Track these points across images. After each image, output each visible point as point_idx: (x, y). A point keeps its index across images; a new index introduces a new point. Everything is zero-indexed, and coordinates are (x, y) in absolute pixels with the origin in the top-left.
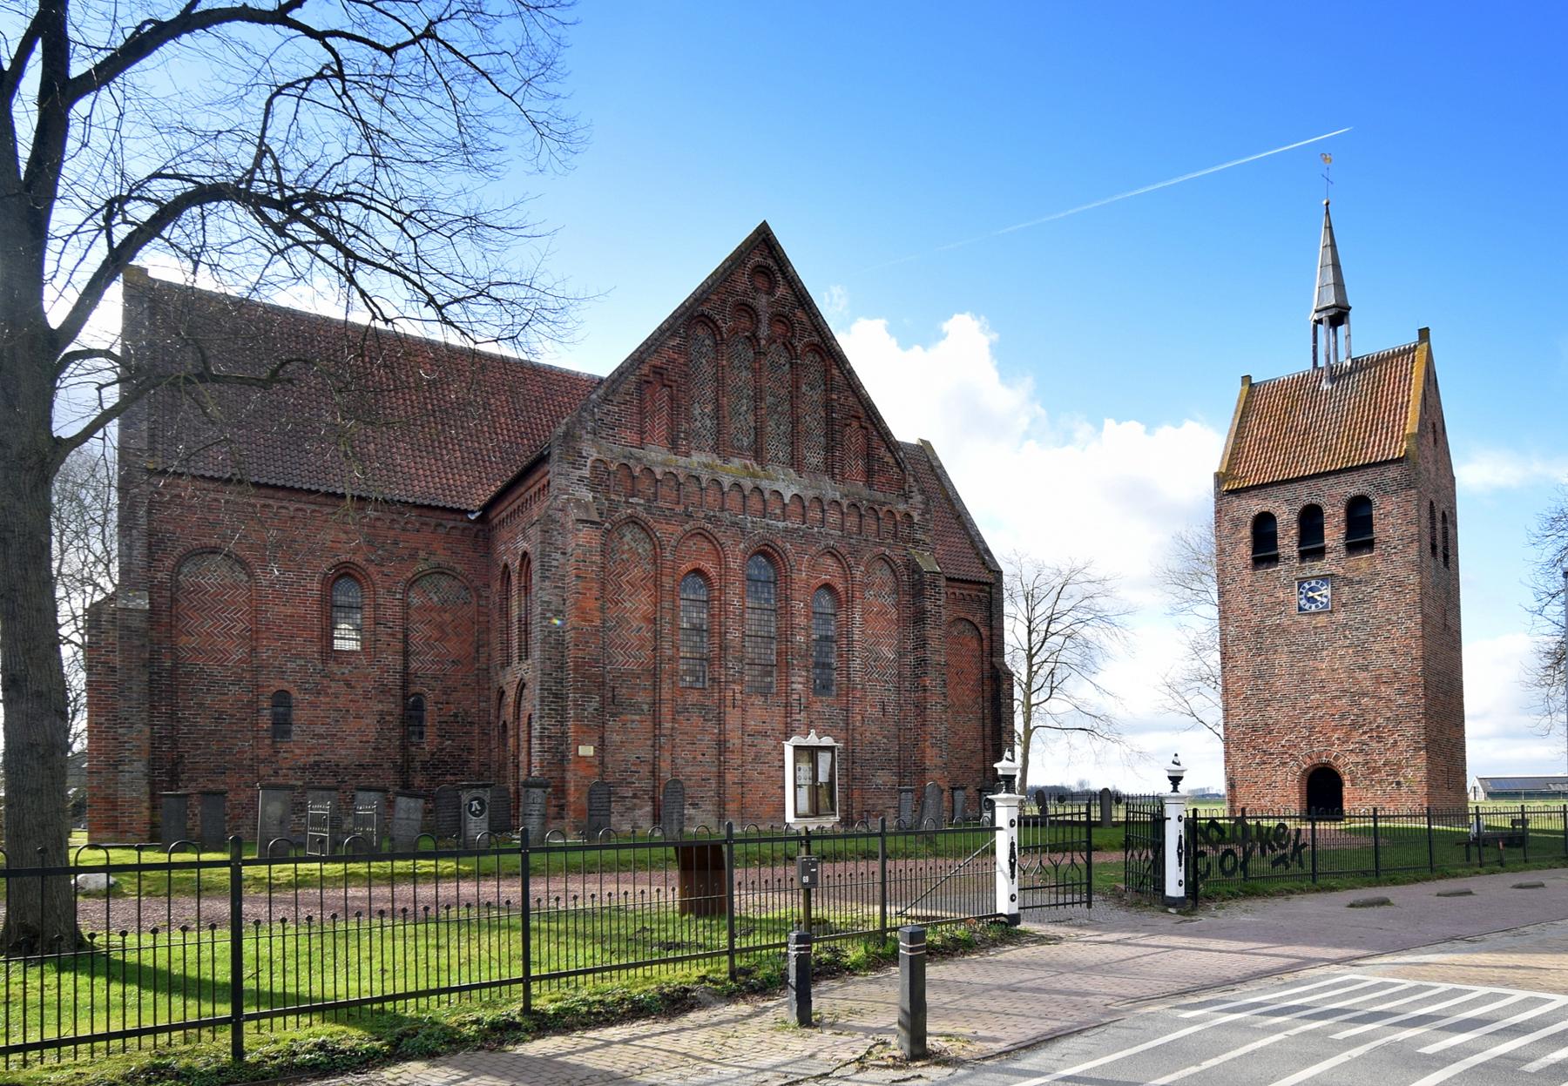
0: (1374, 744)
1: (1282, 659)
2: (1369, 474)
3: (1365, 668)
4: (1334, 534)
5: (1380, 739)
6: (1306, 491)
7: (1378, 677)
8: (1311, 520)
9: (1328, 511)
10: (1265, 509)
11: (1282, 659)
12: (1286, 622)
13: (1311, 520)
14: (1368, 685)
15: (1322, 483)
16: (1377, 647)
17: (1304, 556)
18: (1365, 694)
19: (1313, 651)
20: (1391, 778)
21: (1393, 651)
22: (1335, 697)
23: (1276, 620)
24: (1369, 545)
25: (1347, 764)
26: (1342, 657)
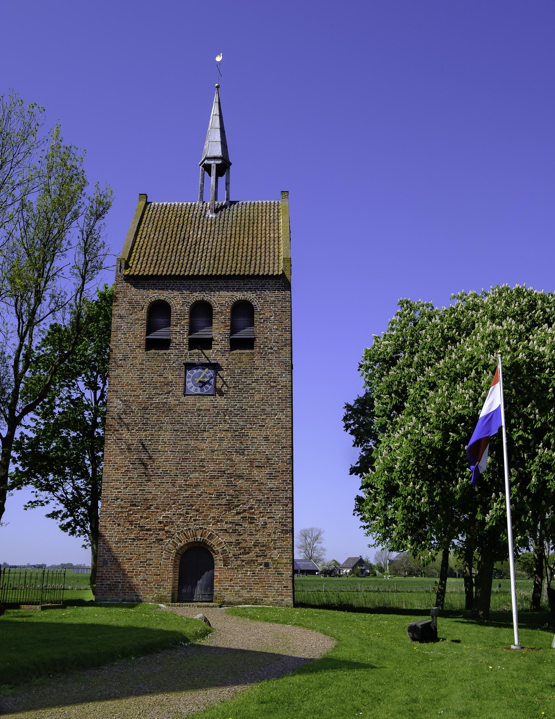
0: (246, 525)
1: (166, 436)
5: (252, 521)
7: (251, 462)
8: (202, 312)
9: (217, 309)
10: (162, 298)
11: (166, 436)
12: (172, 400)
13: (202, 312)
16: (251, 434)
18: (240, 477)
19: (196, 432)
20: (260, 560)
21: (266, 438)
22: (213, 477)
26: (221, 439)
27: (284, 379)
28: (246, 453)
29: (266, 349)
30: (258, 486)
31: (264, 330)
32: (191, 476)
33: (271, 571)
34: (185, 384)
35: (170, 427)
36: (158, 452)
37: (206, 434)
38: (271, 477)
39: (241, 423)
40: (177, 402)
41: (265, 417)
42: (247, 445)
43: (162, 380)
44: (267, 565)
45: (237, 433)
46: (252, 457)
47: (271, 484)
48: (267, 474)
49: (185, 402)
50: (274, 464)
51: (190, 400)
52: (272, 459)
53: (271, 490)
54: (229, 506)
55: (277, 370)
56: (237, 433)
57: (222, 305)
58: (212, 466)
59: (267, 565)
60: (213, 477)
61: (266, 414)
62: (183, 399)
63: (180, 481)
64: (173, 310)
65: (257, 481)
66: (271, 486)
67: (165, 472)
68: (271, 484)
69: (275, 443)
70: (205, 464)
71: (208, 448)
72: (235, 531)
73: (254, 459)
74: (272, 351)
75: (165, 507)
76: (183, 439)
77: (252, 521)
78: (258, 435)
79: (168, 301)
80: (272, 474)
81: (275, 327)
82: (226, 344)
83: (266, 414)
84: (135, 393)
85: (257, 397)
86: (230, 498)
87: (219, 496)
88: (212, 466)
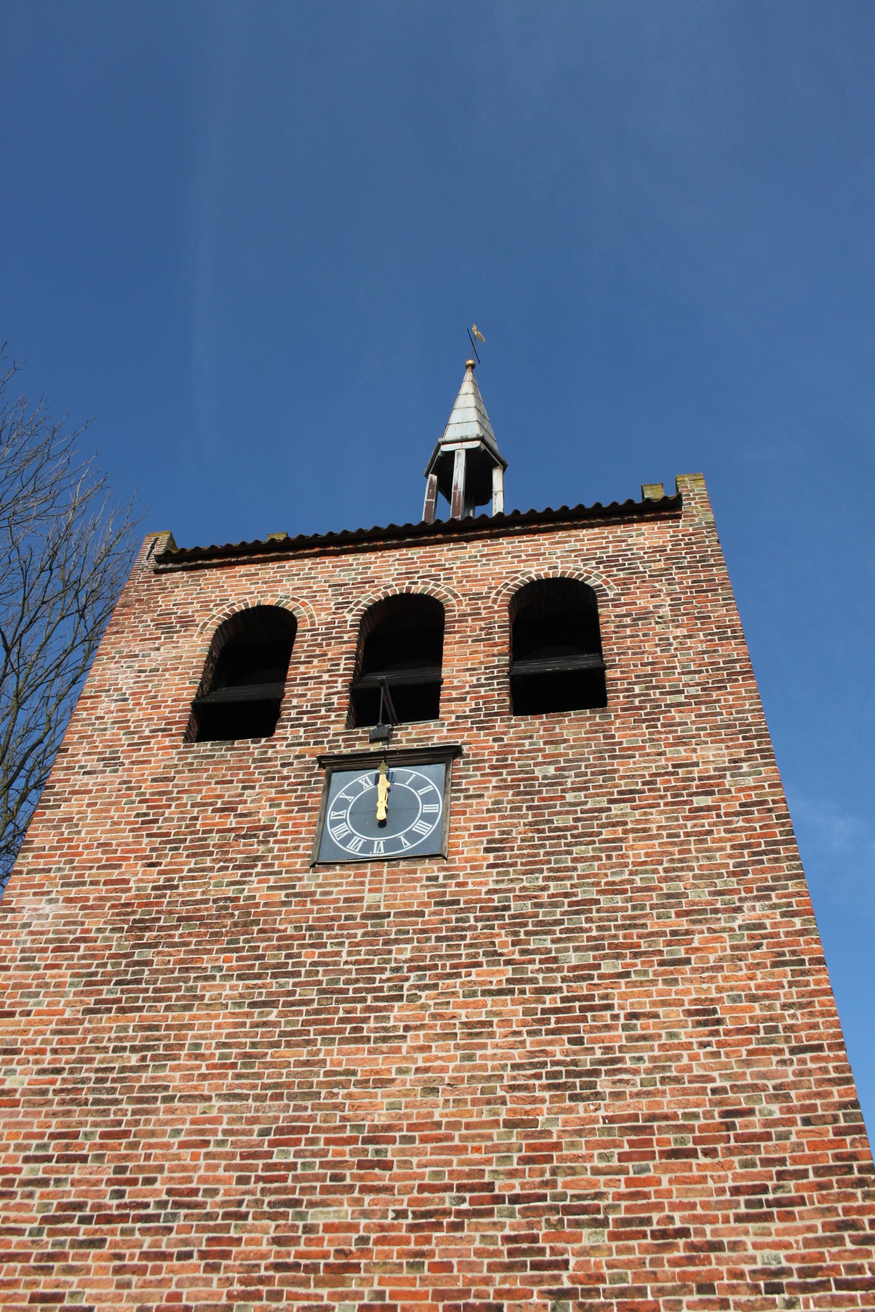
2: (586, 538)
3: (573, 1084)
7: (639, 1130)
12: (257, 888)
14: (593, 1171)
18: (585, 1212)
19: (352, 1007)
21: (705, 1015)
23: (218, 884)
26: (476, 1029)
27: (750, 781)
28: (603, 1084)
29: (655, 694)
30: (690, 1261)
32: (318, 1217)
36: (166, 1099)
37: (397, 1013)
38: (760, 1205)
39: (574, 959)
40: (282, 895)
41: (684, 924)
42: (608, 1050)
43: (232, 822)
45: (550, 1001)
46: (643, 1107)
48: (736, 1191)
49: (313, 894)
50: (767, 1137)
51: (339, 883)
52: (750, 1112)
56: (550, 1001)
60: (427, 1220)
61: (687, 913)
62: (309, 881)
63: (258, 1238)
65: (683, 1233)
66: (764, 1259)
67: (183, 1198)
69: (755, 1031)
70: (391, 1151)
71: (411, 1076)
73: (653, 1118)
74: (681, 698)
76: (292, 1039)
78: (664, 1003)
80: (764, 1189)
83: (687, 913)
84: (115, 874)
88: (422, 1162)
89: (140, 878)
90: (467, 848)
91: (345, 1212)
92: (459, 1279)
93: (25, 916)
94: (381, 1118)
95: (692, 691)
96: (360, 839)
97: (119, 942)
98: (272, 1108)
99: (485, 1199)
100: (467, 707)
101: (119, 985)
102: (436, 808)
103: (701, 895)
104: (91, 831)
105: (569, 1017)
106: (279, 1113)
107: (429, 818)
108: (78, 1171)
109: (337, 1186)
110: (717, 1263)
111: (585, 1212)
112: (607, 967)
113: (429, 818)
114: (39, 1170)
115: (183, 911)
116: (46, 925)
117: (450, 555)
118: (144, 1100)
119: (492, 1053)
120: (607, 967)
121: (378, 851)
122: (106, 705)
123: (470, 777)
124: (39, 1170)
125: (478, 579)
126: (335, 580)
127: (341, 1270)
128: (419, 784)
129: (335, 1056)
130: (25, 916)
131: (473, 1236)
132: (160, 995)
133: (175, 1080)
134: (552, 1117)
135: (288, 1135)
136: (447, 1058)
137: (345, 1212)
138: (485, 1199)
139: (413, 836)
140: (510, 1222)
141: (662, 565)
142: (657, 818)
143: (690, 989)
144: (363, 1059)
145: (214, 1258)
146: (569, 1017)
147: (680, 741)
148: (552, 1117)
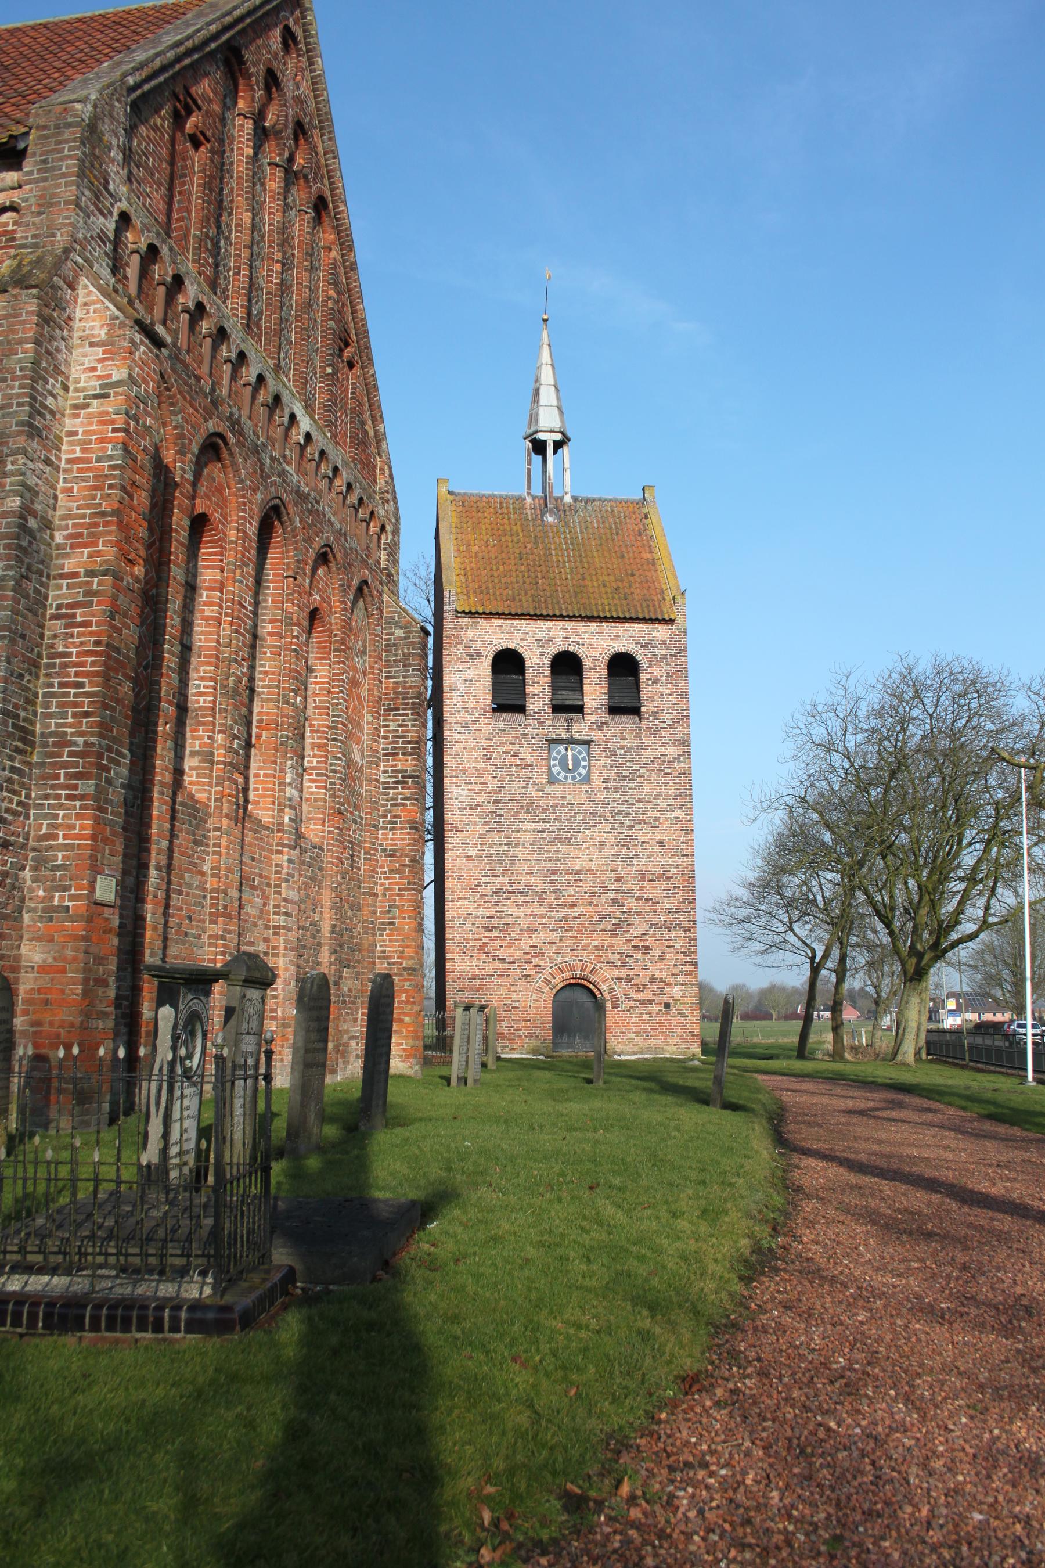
0: (639, 956)
3: (627, 860)
4: (595, 691)
5: (646, 950)
6: (562, 634)
7: (643, 874)
9: (587, 664)
10: (511, 646)
12: (531, 790)
13: (567, 666)
14: (631, 884)
15: (580, 627)
17: (557, 709)
18: (629, 894)
19: (567, 834)
20: (658, 999)
21: (661, 844)
23: (518, 787)
24: (635, 711)
25: (606, 981)
28: (635, 861)
31: (654, 687)
32: (565, 893)
33: (673, 1012)
34: (549, 769)
35: (530, 826)
37: (580, 837)
38: (669, 894)
39: (628, 823)
43: (518, 762)
44: (667, 1006)
45: (622, 836)
46: (644, 868)
47: (668, 903)
53: (669, 910)
54: (615, 931)
55: (672, 752)
56: (622, 836)
57: (595, 659)
58: (590, 880)
59: (667, 1006)
60: (592, 895)
62: (549, 789)
63: (551, 898)
64: (528, 664)
66: (668, 906)
67: (530, 888)
68: (668, 903)
70: (582, 877)
72: (624, 964)
75: (531, 932)
77: (646, 950)
79: (521, 650)
81: (668, 692)
82: (603, 711)
85: (647, 788)
86: (617, 921)
87: (603, 918)
88: (590, 880)
89: (492, 784)
90: (596, 780)
91: (571, 892)
92: (600, 908)
93: (455, 795)
94: (578, 868)
95: (669, 722)
96: (563, 774)
97: (491, 807)
98: (549, 864)
99: (605, 890)
100: (593, 719)
101: (495, 823)
102: (586, 763)
103: (663, 805)
104: (469, 762)
105: (627, 841)
106: (552, 865)
107: (584, 767)
108: (498, 880)
109: (569, 885)
110: (658, 906)
111: (629, 894)
112: (637, 827)
113: (584, 767)
114: (487, 880)
115: (509, 797)
116: (463, 798)
117: (584, 629)
118: (512, 860)
119: (607, 850)
120: (637, 827)
121: (569, 780)
122: (456, 699)
123: (596, 751)
124: (487, 880)
125: (596, 644)
126: (537, 637)
127: (573, 906)
128: (580, 753)
129: (564, 849)
130: (455, 795)
131: (603, 899)
132: (509, 827)
133: (520, 854)
134: (622, 869)
135: (555, 871)
136: (594, 850)
137: (571, 892)
138: (605, 890)
139: (580, 774)
140: (612, 896)
141: (664, 652)
142: (654, 775)
143: (659, 835)
144: (572, 851)
145: (541, 902)
146: (627, 841)
147: (663, 745)
148: (622, 869)
